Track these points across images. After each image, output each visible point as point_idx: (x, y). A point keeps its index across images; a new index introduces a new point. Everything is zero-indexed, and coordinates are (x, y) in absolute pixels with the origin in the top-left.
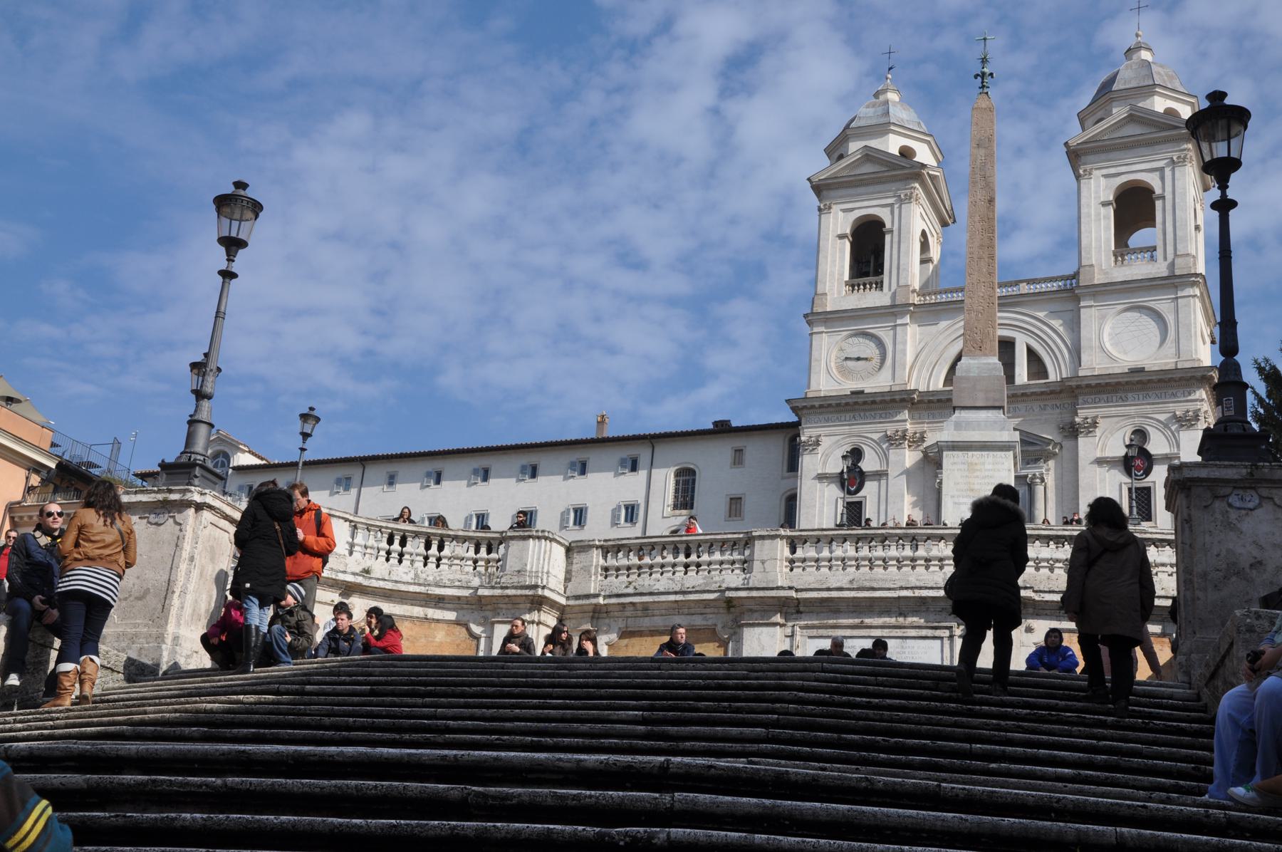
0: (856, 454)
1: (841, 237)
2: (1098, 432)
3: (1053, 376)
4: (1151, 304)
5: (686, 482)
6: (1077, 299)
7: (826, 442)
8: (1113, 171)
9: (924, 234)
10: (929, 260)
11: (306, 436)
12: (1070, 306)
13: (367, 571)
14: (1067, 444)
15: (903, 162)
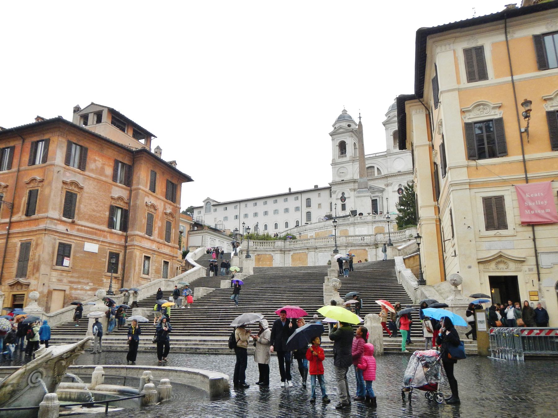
0: (343, 193)
1: (337, 146)
2: (393, 185)
3: (383, 174)
4: (401, 157)
5: (309, 201)
6: (387, 156)
7: (337, 191)
8: (392, 128)
9: (355, 143)
10: (357, 148)
11: (243, 226)
12: (385, 158)
13: (256, 248)
14: (386, 188)
15: (349, 128)
